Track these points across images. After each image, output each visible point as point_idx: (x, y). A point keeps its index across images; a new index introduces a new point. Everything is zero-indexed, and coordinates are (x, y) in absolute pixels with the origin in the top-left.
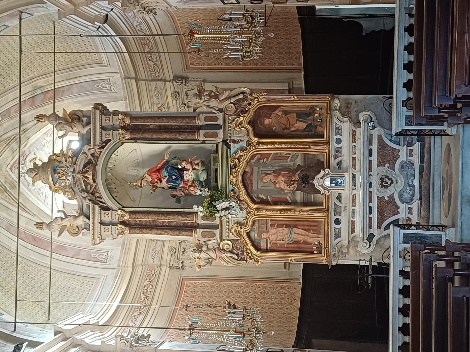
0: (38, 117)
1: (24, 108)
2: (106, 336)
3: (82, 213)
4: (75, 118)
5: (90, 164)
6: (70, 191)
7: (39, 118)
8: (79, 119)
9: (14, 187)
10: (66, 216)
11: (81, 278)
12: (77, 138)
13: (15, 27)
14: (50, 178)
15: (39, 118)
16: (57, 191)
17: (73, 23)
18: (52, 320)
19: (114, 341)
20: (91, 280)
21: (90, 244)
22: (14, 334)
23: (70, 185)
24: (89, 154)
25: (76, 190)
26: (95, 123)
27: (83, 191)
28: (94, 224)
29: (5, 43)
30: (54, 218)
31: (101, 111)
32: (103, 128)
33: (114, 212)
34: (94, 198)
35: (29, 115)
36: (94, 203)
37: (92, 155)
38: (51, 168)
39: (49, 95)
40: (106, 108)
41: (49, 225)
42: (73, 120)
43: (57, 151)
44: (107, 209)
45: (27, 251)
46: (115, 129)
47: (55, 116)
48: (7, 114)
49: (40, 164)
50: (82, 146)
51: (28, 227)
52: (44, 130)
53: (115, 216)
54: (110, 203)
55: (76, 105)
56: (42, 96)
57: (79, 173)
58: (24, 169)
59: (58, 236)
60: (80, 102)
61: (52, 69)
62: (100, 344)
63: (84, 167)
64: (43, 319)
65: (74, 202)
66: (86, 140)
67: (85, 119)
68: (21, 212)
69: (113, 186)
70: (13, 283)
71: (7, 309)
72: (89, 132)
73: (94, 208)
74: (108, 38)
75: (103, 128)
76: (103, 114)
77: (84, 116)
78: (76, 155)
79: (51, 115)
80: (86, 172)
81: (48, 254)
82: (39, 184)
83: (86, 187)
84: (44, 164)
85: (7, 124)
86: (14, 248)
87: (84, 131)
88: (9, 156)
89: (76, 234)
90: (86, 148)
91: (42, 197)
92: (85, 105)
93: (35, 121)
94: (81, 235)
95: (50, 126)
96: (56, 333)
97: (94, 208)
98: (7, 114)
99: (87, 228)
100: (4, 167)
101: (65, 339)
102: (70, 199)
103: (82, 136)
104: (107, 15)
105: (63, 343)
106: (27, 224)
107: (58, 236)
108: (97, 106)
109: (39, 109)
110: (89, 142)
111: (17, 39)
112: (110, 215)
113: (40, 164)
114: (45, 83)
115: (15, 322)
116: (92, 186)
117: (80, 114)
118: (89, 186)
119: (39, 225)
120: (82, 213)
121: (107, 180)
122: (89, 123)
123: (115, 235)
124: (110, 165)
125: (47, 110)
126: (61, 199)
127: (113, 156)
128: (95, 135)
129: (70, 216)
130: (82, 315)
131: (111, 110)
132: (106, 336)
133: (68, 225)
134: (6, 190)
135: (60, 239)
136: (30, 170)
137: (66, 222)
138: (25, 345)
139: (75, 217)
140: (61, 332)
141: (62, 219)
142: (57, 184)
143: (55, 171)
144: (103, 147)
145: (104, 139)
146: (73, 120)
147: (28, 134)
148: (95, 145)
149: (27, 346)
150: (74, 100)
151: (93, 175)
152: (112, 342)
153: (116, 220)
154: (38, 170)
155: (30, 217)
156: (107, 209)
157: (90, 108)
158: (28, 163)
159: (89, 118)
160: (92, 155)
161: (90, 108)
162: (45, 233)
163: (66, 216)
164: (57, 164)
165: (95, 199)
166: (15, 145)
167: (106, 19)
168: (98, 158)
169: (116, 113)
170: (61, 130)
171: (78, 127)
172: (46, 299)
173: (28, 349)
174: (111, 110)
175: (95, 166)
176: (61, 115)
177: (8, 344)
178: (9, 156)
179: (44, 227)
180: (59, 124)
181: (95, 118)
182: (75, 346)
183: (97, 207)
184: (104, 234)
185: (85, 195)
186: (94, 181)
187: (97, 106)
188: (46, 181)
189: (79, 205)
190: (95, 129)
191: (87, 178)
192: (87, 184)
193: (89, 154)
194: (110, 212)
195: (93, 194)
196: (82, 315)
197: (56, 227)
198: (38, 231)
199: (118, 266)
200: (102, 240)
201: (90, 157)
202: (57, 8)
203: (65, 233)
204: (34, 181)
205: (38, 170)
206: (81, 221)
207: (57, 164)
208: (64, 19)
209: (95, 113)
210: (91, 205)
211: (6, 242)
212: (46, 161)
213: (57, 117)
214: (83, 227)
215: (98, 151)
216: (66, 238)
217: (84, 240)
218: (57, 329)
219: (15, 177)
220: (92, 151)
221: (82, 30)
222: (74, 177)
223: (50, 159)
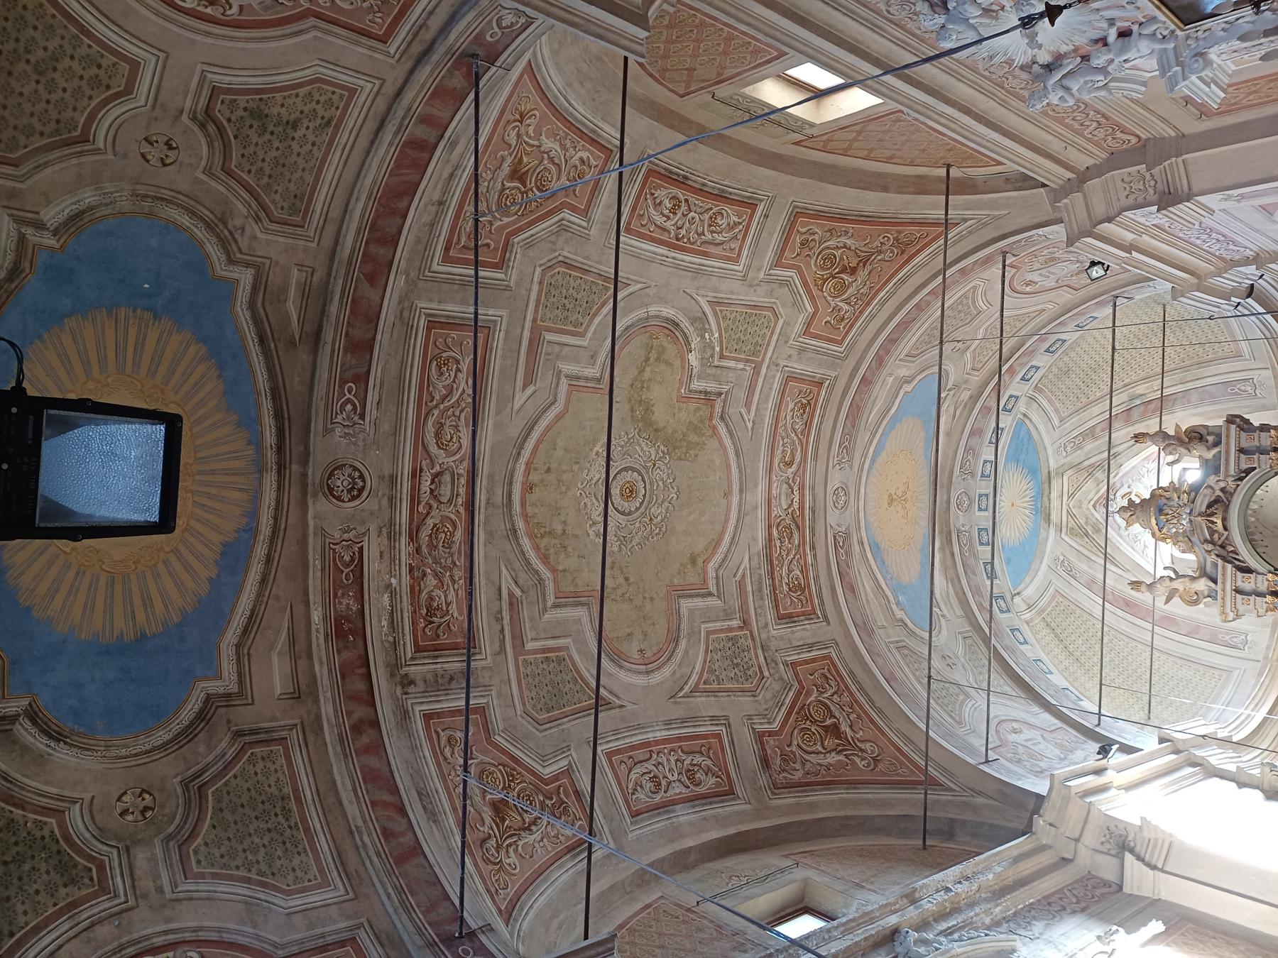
0: (1136, 436)
1: (1115, 425)
2: (1244, 759)
3: (1203, 573)
4: (1195, 437)
5: (1220, 503)
6: (1186, 540)
7: (1139, 437)
8: (1201, 438)
9: (1098, 531)
10: (1178, 576)
11: (1201, 668)
12: (1197, 465)
13: (1107, 317)
14: (1153, 521)
15: (1139, 437)
16: (1164, 540)
17: (1198, 303)
18: (1154, 722)
19: (1258, 771)
20: (1217, 673)
21: (1217, 620)
22: (1097, 729)
23: (1185, 532)
24: (1217, 488)
25: (1195, 539)
26: (1228, 444)
27: (1206, 541)
28: (1224, 590)
29: (1090, 340)
30: (1158, 576)
31: (1238, 426)
32: (1241, 451)
33: (1260, 577)
34: (1225, 554)
35: (1122, 434)
36: (1224, 559)
37: (1223, 490)
38: (1157, 508)
39: (1152, 406)
40: (1247, 422)
41: (1150, 587)
42: (1190, 439)
43: (1164, 483)
44: (1248, 570)
45: (1115, 617)
46: (1263, 452)
47: (1162, 435)
48: (1091, 433)
49: (1138, 501)
50: (1206, 476)
51: (1119, 587)
52: (1144, 454)
53: (1263, 582)
54: (1252, 562)
55: (1195, 418)
56: (1142, 408)
57: (1200, 515)
58: (1114, 507)
59: (1167, 601)
60: (1200, 414)
61: (1159, 370)
62: (1234, 770)
63: (1209, 506)
64: (1141, 716)
65: (1191, 557)
66: (1212, 467)
67: (1211, 438)
68: (1108, 565)
69: (1257, 537)
70: (1096, 659)
71: (1088, 694)
72: (1217, 457)
73: (1224, 568)
74: (1253, 318)
75: (1241, 451)
76: (1242, 429)
77: (1209, 434)
78: (1195, 490)
79: (1156, 433)
80: (1213, 514)
81: (1149, 626)
82: (1137, 528)
83: (1211, 535)
84: (1143, 501)
85: (1090, 446)
86: (1097, 611)
87: (1210, 455)
88: (1092, 490)
89: (1196, 603)
90: (1212, 480)
91: (1139, 547)
92: (1211, 418)
93: (1132, 442)
94: (1201, 606)
95: (1154, 449)
96: (1162, 741)
97: (1224, 568)
98: (1091, 433)
99: (1212, 595)
100: (1085, 503)
101: (1177, 752)
102: (1183, 552)
103: (1205, 462)
104: (1252, 286)
105: (1173, 757)
106: (1117, 582)
107: (1167, 601)
108: (1231, 420)
109: (1136, 426)
110: (1217, 471)
111: (1109, 333)
112: (1252, 580)
113: (1138, 501)
114: (1149, 390)
115: (1100, 714)
116: (1220, 535)
117: (1204, 432)
118: (1216, 536)
119: (1136, 585)
120: (1203, 573)
121: (1247, 527)
122: (1217, 444)
123: (1262, 611)
124: (1253, 506)
125: (1151, 426)
126: (1168, 551)
127: (1259, 492)
128: (1227, 460)
129: (1184, 576)
130: (1203, 722)
131: (1256, 424)
132: (1244, 759)
133: (1181, 588)
134: (1087, 535)
135: (1166, 607)
136: (1123, 509)
137: (1177, 584)
138: (1115, 747)
139: (1193, 579)
140: (1168, 741)
141: (1171, 579)
142: (1164, 530)
143: (1161, 511)
144: (1241, 479)
145: (1244, 466)
146: (1190, 439)
147: (1119, 460)
148: (1227, 476)
149: (1118, 750)
150: (1193, 411)
151: (1224, 520)
152: (1256, 772)
153: (1263, 587)
154: (1134, 509)
155: (1120, 572)
156: (1248, 570)
157: (1220, 422)
158: (1119, 499)
159: (1219, 436)
160: (1223, 490)
161: (1220, 422)
162: (1144, 597)
163: (1178, 576)
164: (1164, 501)
165: (1226, 553)
166: (1101, 475)
167: (1250, 291)
168: (1232, 495)
169: (1264, 428)
170: (1171, 453)
171: (1199, 450)
172: (1146, 689)
173: (1118, 754)
174: (1256, 424)
175: (1226, 508)
176: (1171, 432)
177: (1090, 742)
178: (1092, 490)
179: (1143, 588)
180: (1168, 445)
181: (1228, 436)
182: (1194, 765)
183: (1229, 566)
184: (1241, 608)
185: (1210, 547)
186: (1225, 528)
187: (1231, 420)
188: (1146, 525)
189: (1199, 562)
190: (1227, 452)
191: (1213, 523)
192: (1212, 532)
193: (1217, 488)
194: (1253, 576)
195: (1222, 547)
196: (1203, 722)
197: (1161, 590)
198: (1133, 593)
199: (1266, 658)
200: (1238, 616)
201: (1218, 493)
202: (1169, 286)
203: (1176, 600)
204: (1129, 524)
205: (1134, 509)
206: (1202, 585)
207: (1164, 501)
208: (1182, 299)
209: (1228, 429)
210: (1220, 562)
211: (1086, 604)
212: (1148, 497)
213: (1165, 436)
214: (1206, 593)
215: (1232, 485)
216: (1177, 607)
217: (1206, 613)
218: (1163, 735)
219: (1099, 516)
220: (1222, 485)
221: (1207, 310)
222: (1191, 521)
223: (1153, 494)
